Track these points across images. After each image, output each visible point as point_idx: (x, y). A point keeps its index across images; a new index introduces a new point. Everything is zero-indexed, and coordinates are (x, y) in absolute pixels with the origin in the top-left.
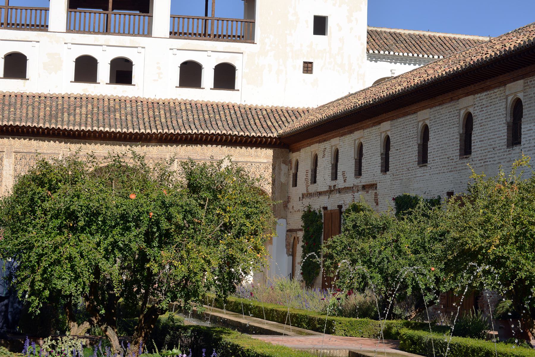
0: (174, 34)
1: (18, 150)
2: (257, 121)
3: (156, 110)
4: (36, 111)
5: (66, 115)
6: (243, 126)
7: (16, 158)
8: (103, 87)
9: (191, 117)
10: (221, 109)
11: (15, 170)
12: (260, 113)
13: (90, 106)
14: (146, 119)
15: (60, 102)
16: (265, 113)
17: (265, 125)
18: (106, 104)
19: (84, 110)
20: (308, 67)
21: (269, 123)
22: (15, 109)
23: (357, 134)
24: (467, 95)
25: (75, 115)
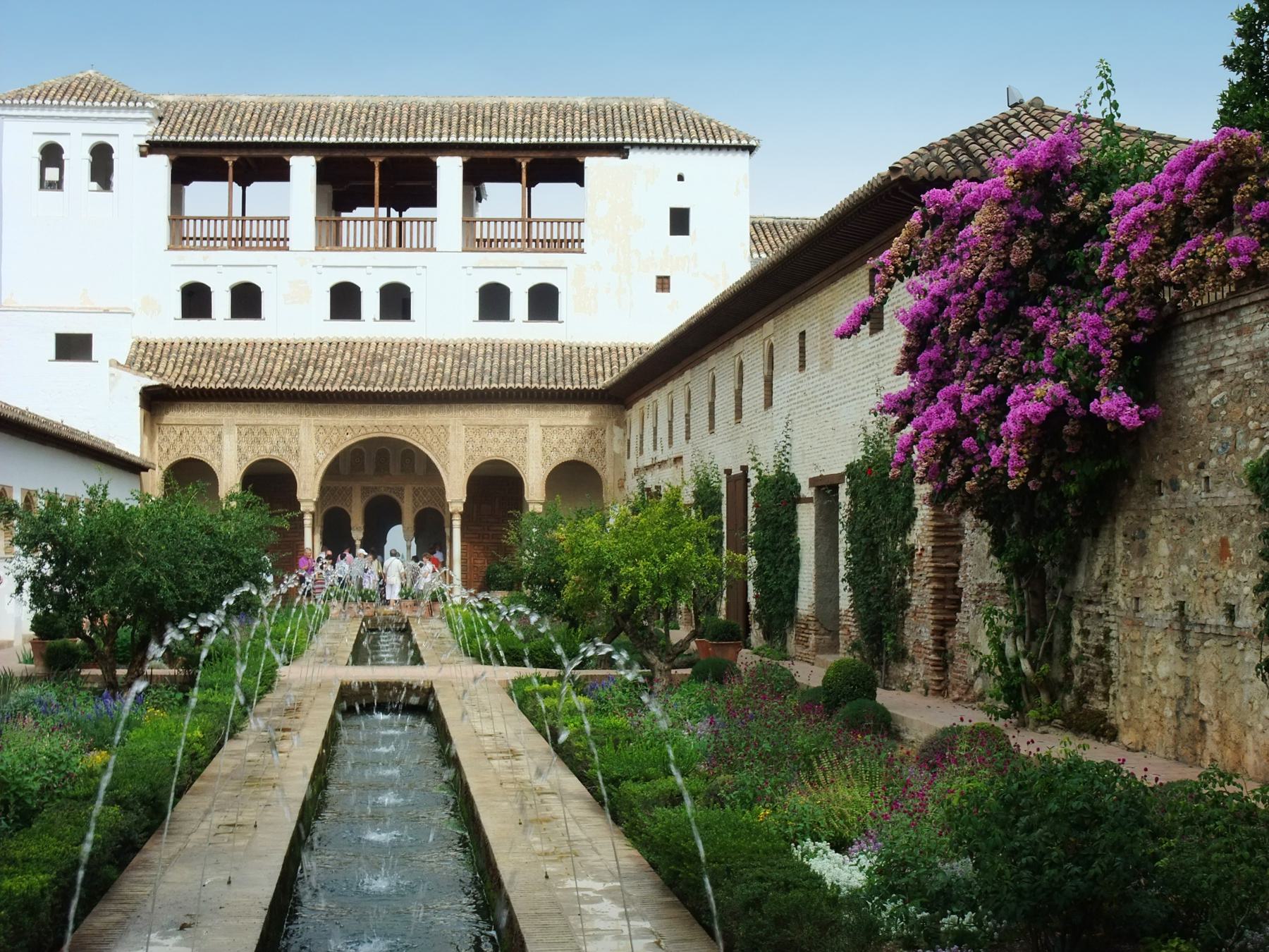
0: (474, 243)
1: (242, 422)
2: (584, 366)
3: (441, 357)
4: (270, 364)
5: (311, 368)
6: (560, 375)
7: (240, 433)
8: (370, 326)
9: (488, 365)
10: (536, 349)
11: (239, 450)
12: (591, 353)
13: (348, 354)
14: (424, 371)
15: (307, 351)
16: (598, 352)
17: (592, 372)
18: (372, 349)
19: (338, 361)
20: (663, 283)
21: (600, 369)
22: (241, 363)
23: (669, 386)
24: (741, 335)
25: (323, 368)
